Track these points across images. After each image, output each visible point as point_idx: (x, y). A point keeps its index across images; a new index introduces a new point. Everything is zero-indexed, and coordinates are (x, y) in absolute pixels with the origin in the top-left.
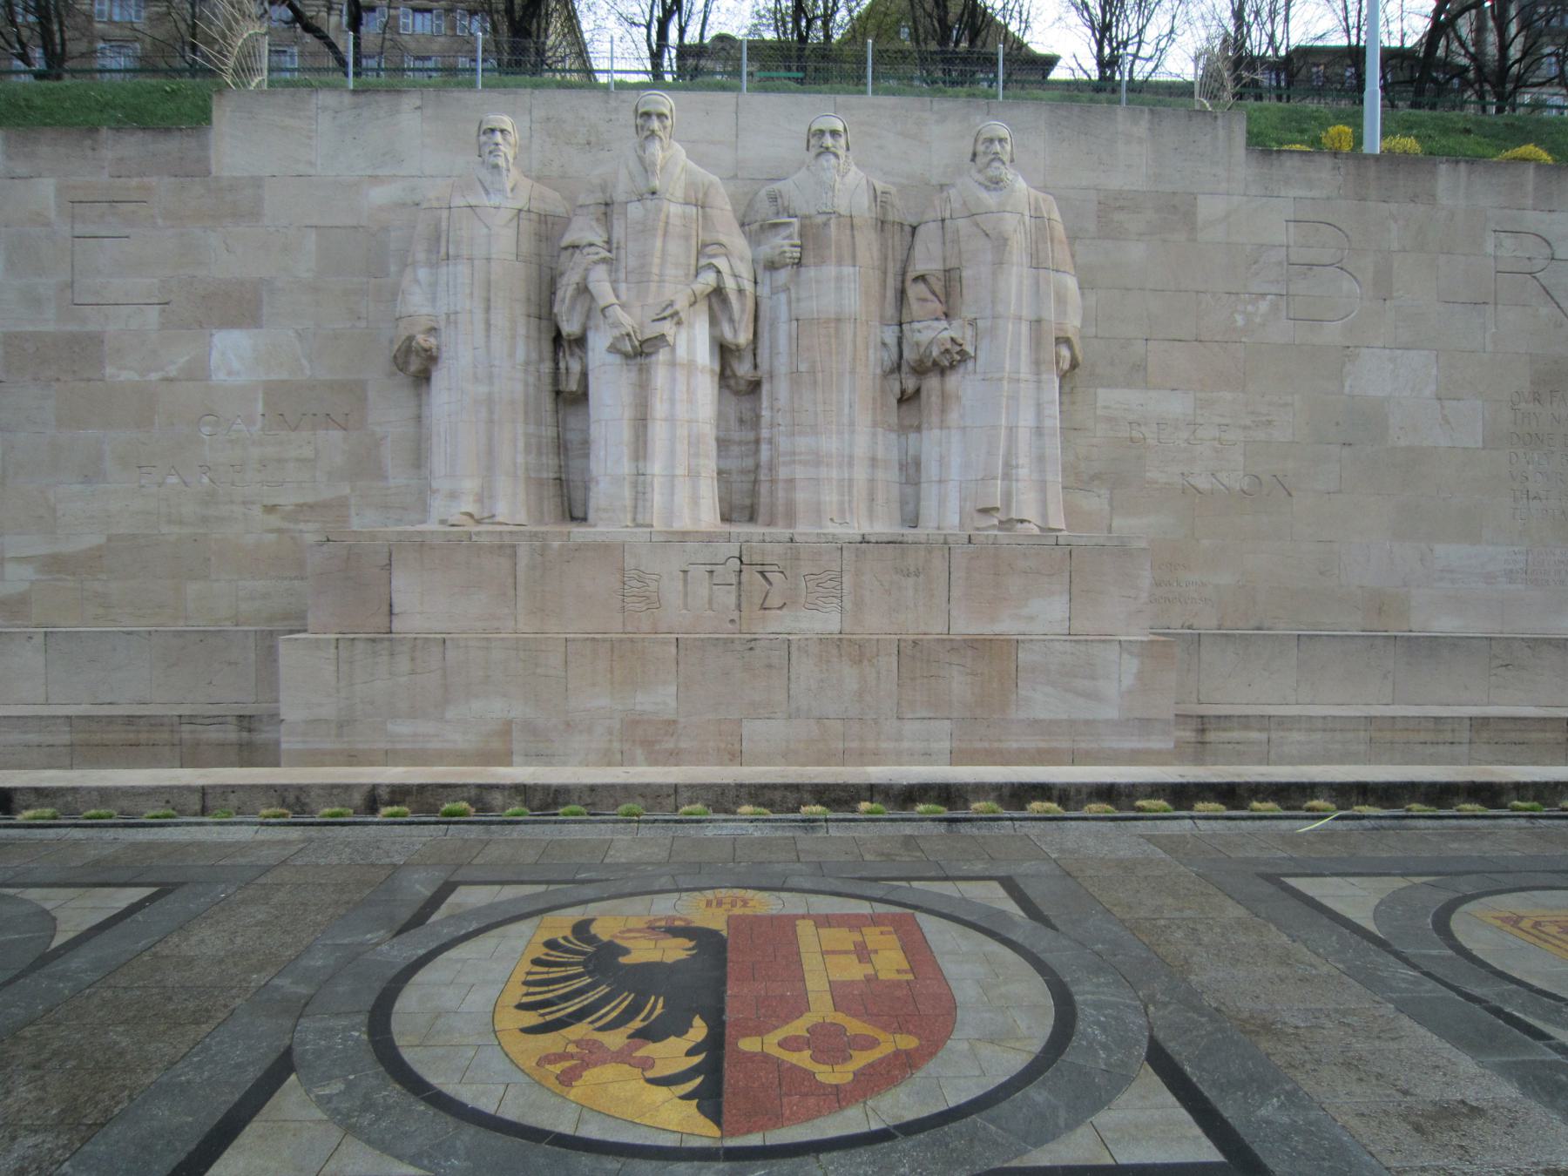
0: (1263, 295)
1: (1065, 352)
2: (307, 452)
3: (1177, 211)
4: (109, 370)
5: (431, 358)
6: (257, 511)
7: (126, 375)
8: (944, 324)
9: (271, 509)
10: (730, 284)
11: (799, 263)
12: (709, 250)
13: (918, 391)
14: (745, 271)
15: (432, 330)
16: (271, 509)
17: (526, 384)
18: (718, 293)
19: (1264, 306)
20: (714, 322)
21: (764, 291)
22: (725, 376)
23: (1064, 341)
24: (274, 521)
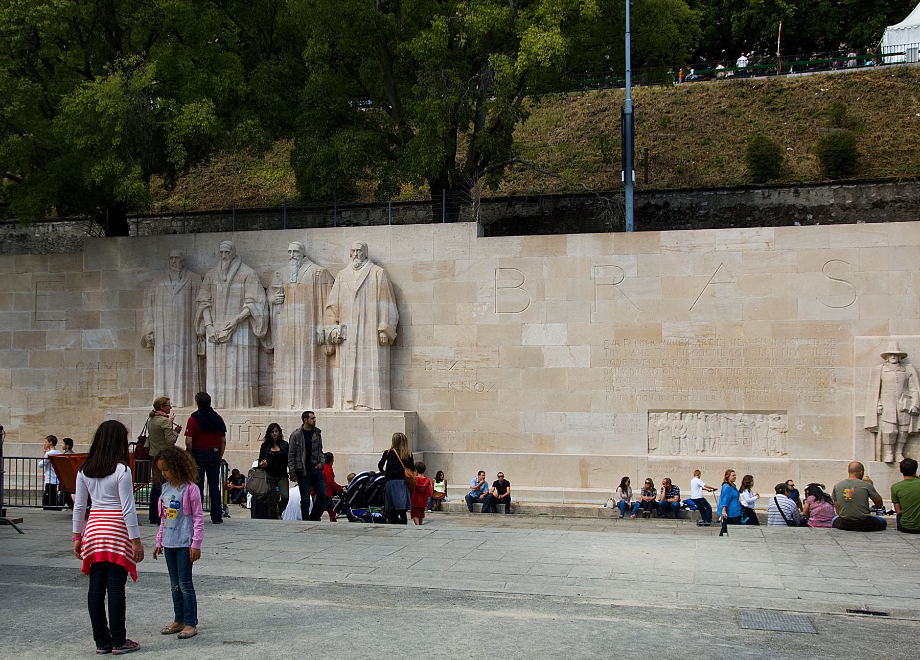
0: (485, 303)
1: (382, 335)
2: (114, 377)
3: (447, 269)
4: (47, 346)
5: (152, 343)
6: (96, 399)
7: (53, 348)
8: (335, 326)
9: (101, 399)
10: (255, 314)
11: (283, 302)
12: (247, 301)
13: (334, 353)
14: (260, 307)
15: (152, 333)
16: (101, 399)
17: (184, 353)
18: (249, 318)
19: (485, 308)
20: (250, 328)
21: (273, 314)
22: (260, 348)
23: (383, 331)
24: (102, 403)
